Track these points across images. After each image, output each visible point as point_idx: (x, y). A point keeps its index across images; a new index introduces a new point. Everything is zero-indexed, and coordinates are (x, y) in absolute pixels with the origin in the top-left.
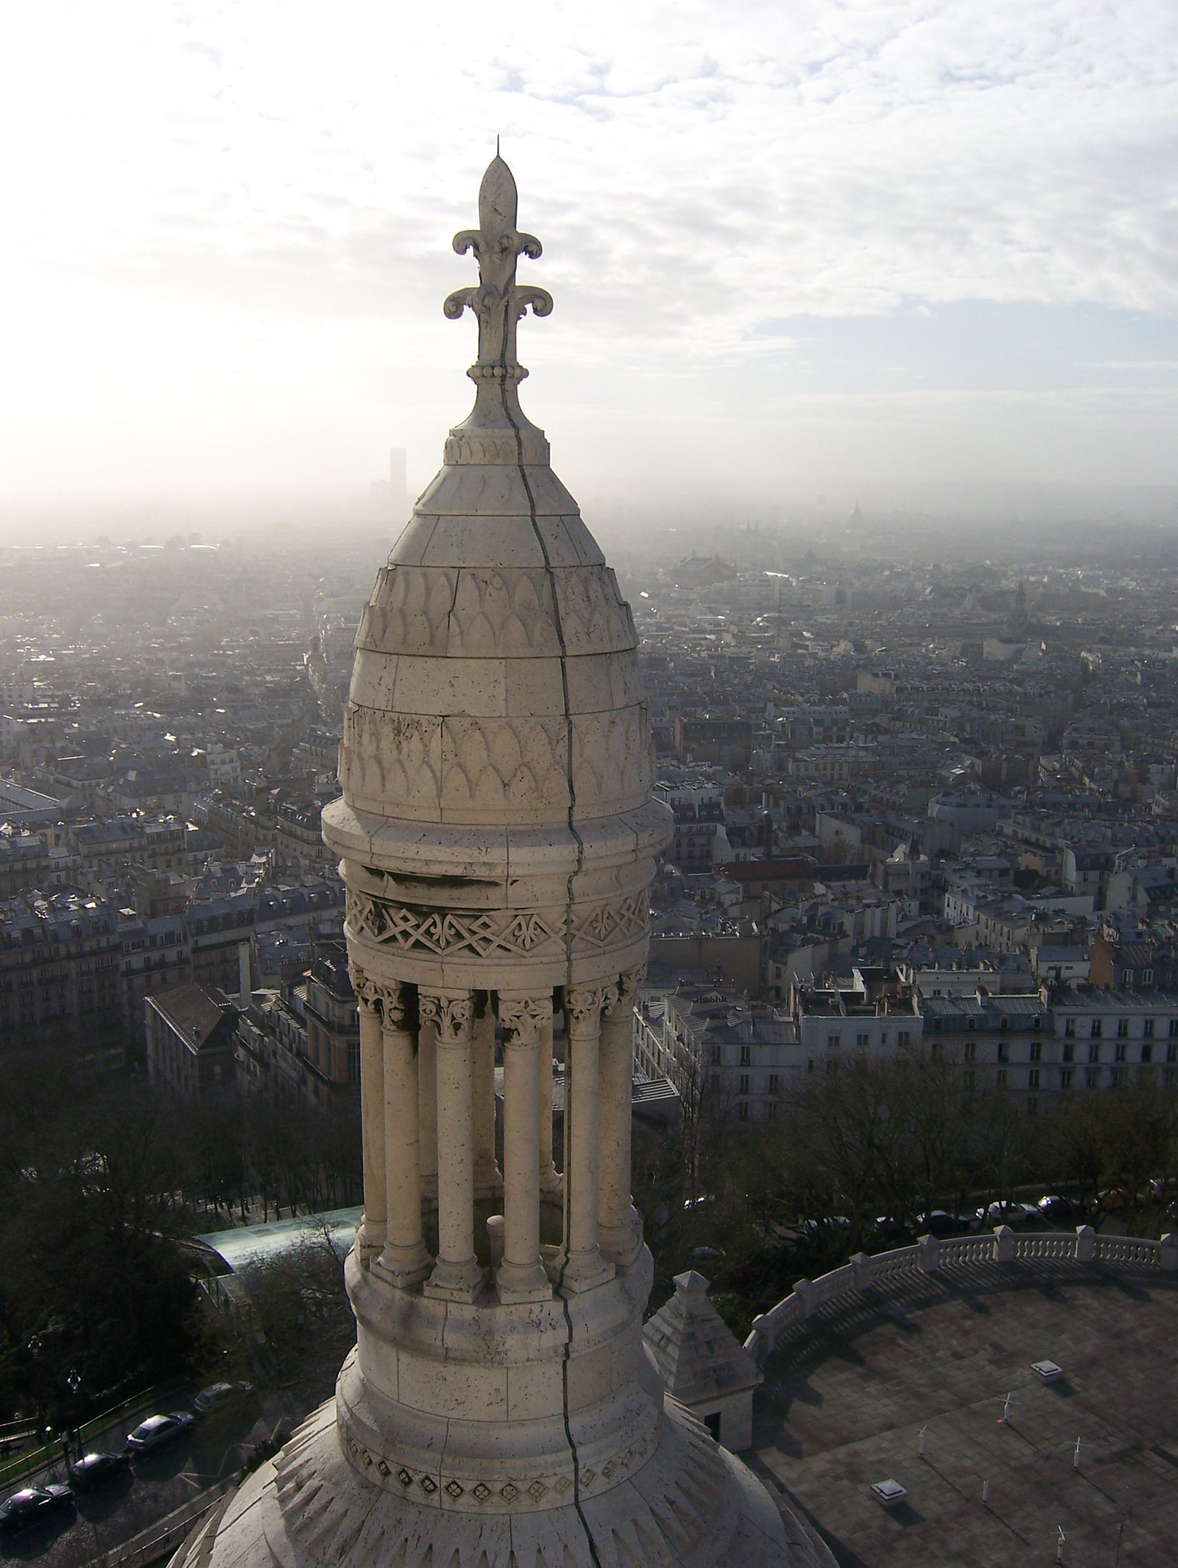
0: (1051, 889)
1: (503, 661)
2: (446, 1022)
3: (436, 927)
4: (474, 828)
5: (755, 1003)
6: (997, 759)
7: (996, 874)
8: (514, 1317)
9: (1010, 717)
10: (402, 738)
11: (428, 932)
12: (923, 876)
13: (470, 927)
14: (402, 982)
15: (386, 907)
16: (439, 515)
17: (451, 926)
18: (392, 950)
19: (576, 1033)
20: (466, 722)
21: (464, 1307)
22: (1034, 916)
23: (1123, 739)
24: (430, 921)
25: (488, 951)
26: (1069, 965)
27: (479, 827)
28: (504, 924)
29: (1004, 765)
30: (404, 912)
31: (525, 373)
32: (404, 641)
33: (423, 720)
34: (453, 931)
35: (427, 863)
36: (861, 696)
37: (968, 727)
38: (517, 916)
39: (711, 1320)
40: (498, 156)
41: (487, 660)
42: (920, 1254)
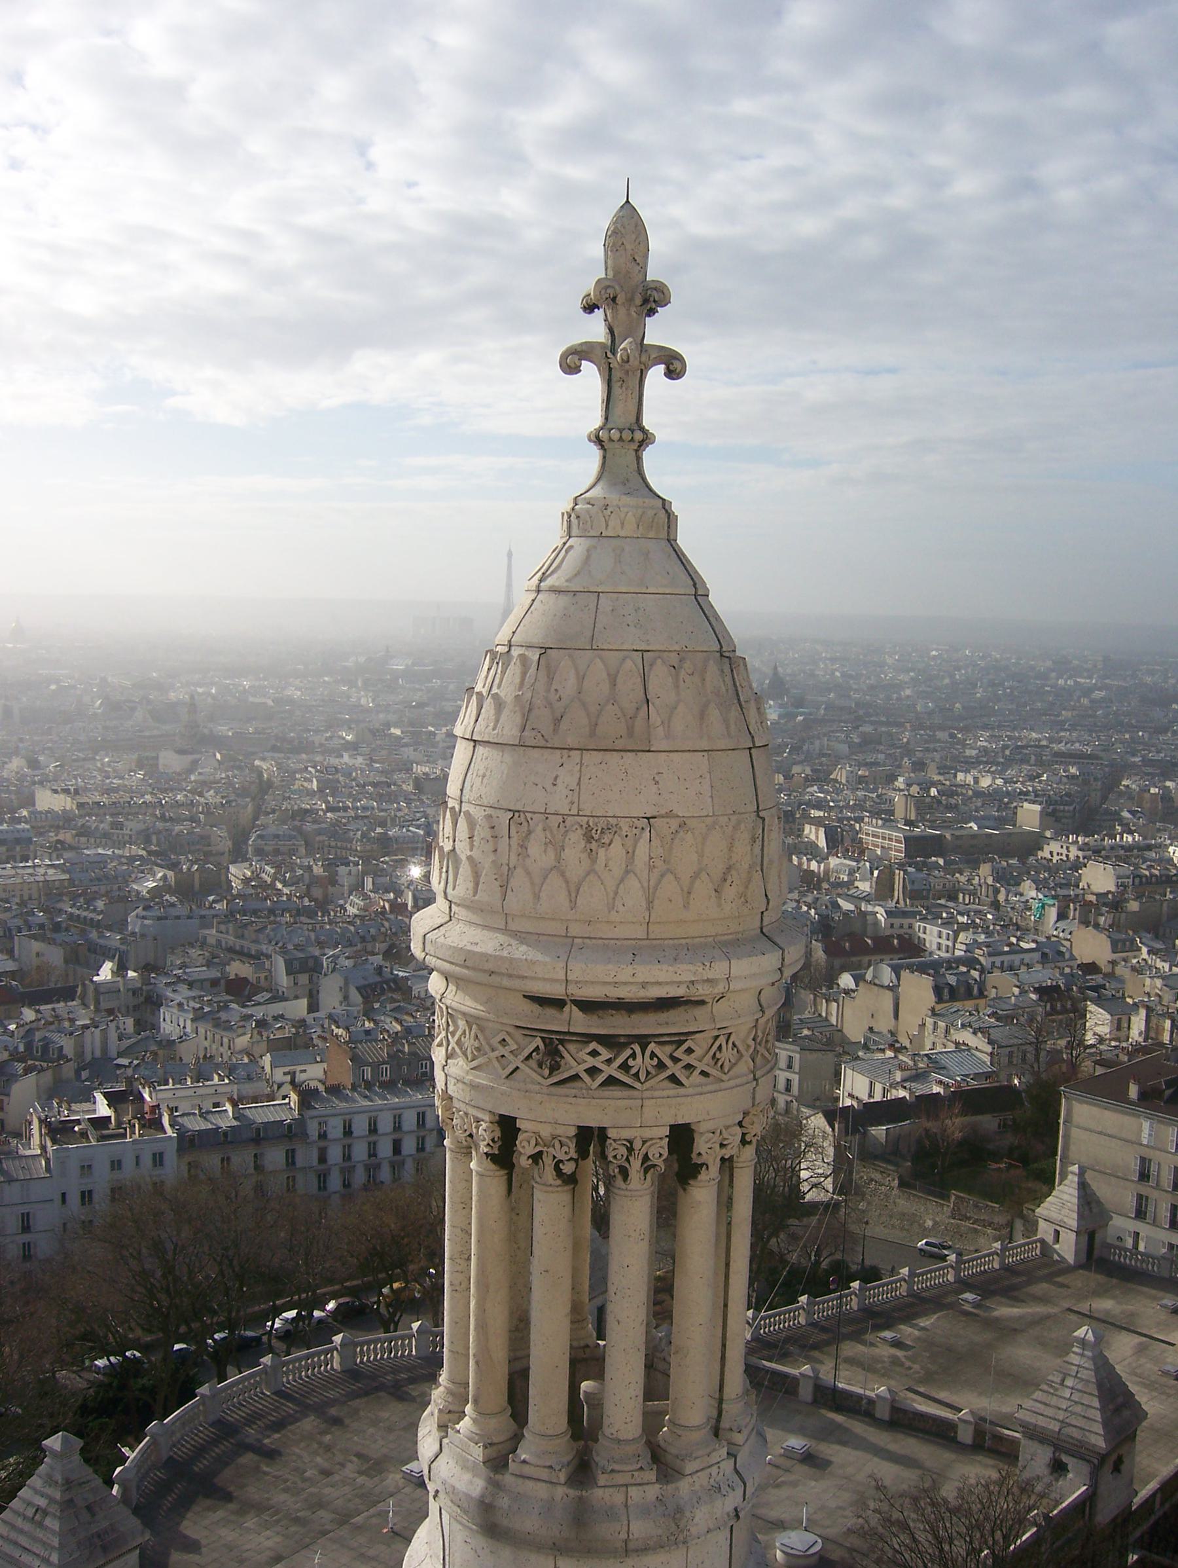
1: (705, 754)
2: (636, 1165)
3: (634, 1059)
4: (683, 941)
6: (189, 869)
7: (207, 985)
8: (697, 1487)
9: (195, 828)
10: (594, 845)
11: (625, 1067)
12: (134, 994)
13: (675, 1054)
15: (562, 1042)
17: (653, 1055)
18: (574, 1092)
19: (740, 1160)
20: (674, 823)
21: (646, 1488)
22: (254, 1023)
23: (307, 844)
24: (628, 1052)
27: (687, 941)
28: (705, 1046)
29: (197, 876)
30: (593, 1045)
32: (593, 734)
33: (624, 826)
34: (655, 1061)
35: (644, 985)
36: (41, 812)
37: (154, 839)
39: (88, 1482)
40: (627, 201)
41: (691, 753)
42: (263, 1376)
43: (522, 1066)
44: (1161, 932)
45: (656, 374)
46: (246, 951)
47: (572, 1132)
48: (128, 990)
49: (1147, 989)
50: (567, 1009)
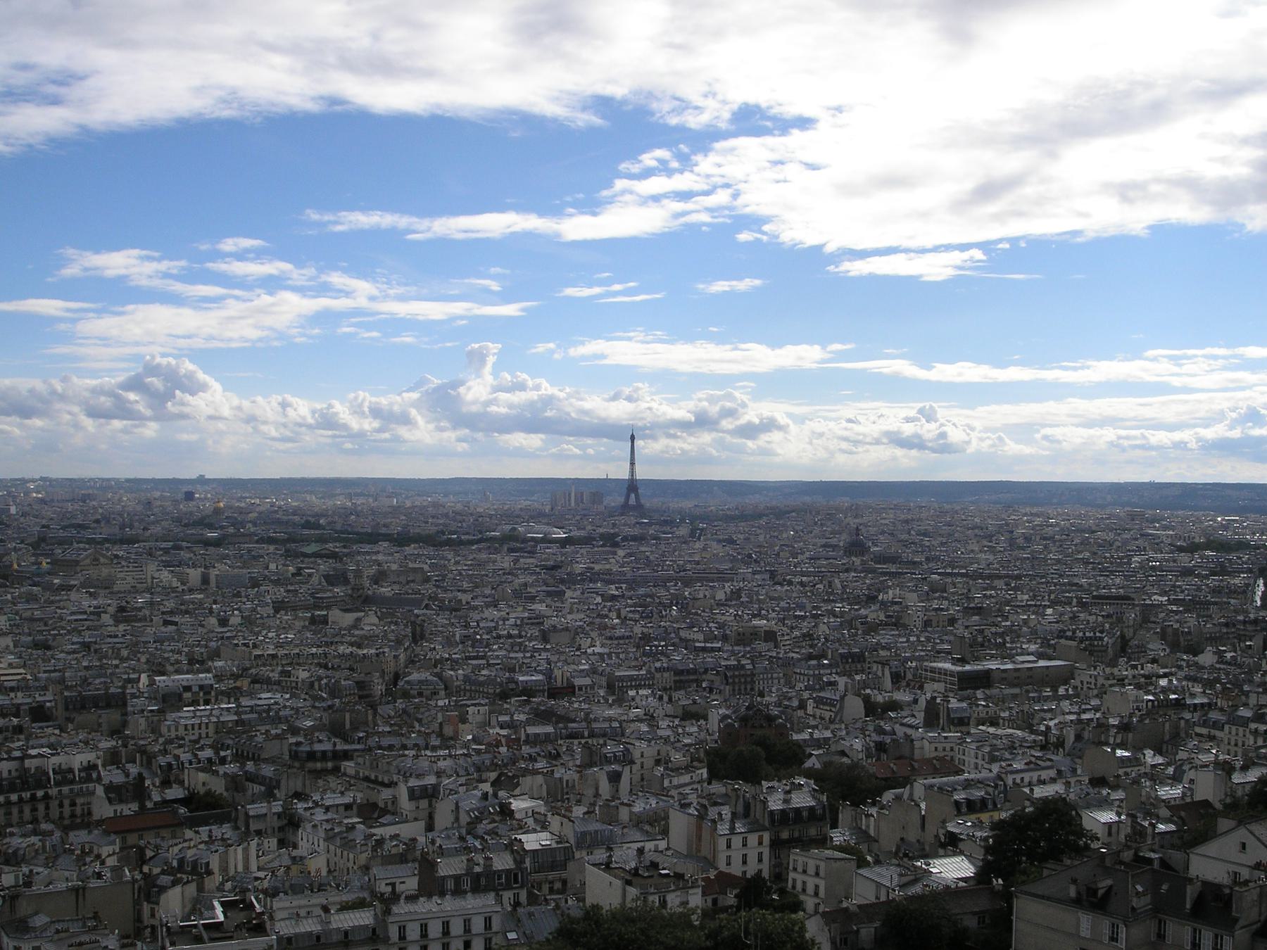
5: (125, 941)
7: (342, 809)
12: (279, 817)
23: (446, 688)
29: (347, 716)
44: (1164, 750)
46: (380, 780)
48: (274, 814)
49: (1143, 799)
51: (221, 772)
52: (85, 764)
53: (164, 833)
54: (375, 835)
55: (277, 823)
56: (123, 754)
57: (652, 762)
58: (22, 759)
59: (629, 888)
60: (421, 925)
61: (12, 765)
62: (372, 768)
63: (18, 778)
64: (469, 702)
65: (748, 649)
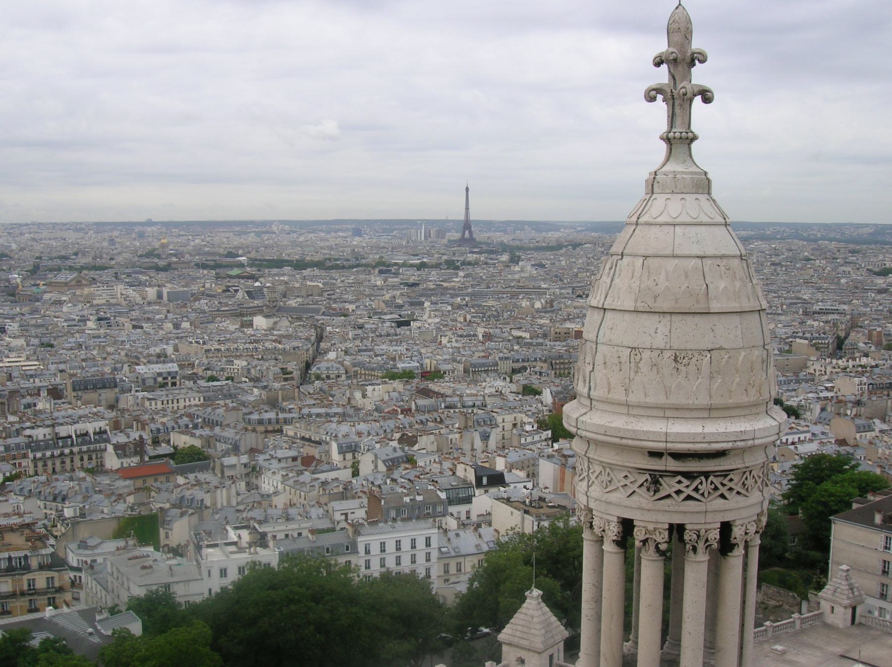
0: (325, 467)
2: (701, 546)
11: (696, 489)
12: (245, 467)
14: (670, 524)
15: (661, 476)
16: (674, 225)
17: (712, 482)
23: (347, 372)
24: (698, 481)
25: (732, 496)
26: (353, 511)
30: (679, 478)
31: (695, 138)
38: (745, 472)
40: (680, 4)
43: (637, 490)
44: (887, 420)
45: (698, 99)
46: (313, 439)
47: (667, 526)
48: (242, 464)
49: (880, 456)
50: (664, 457)
51: (198, 435)
52: (98, 430)
53: (162, 478)
54: (318, 479)
55: (245, 471)
56: (123, 424)
57: (511, 426)
58: (53, 426)
59: (526, 516)
60: (381, 543)
61: (48, 430)
62: (307, 430)
63: (50, 440)
64: (367, 383)
65: (564, 343)
